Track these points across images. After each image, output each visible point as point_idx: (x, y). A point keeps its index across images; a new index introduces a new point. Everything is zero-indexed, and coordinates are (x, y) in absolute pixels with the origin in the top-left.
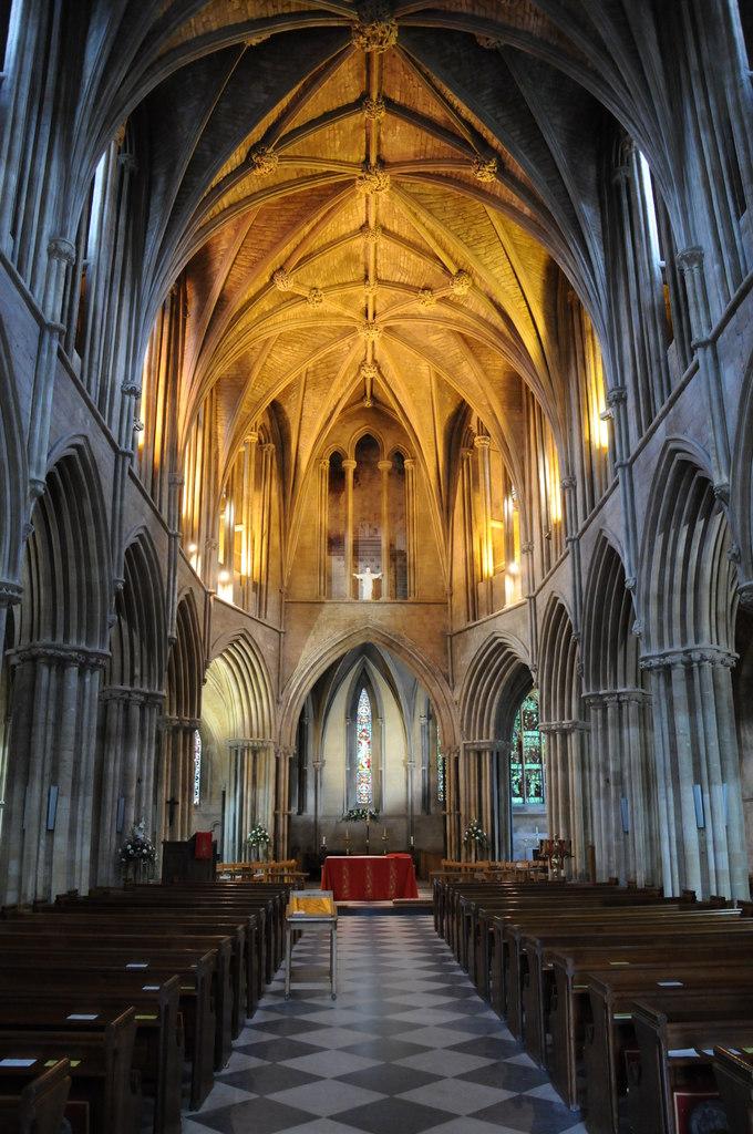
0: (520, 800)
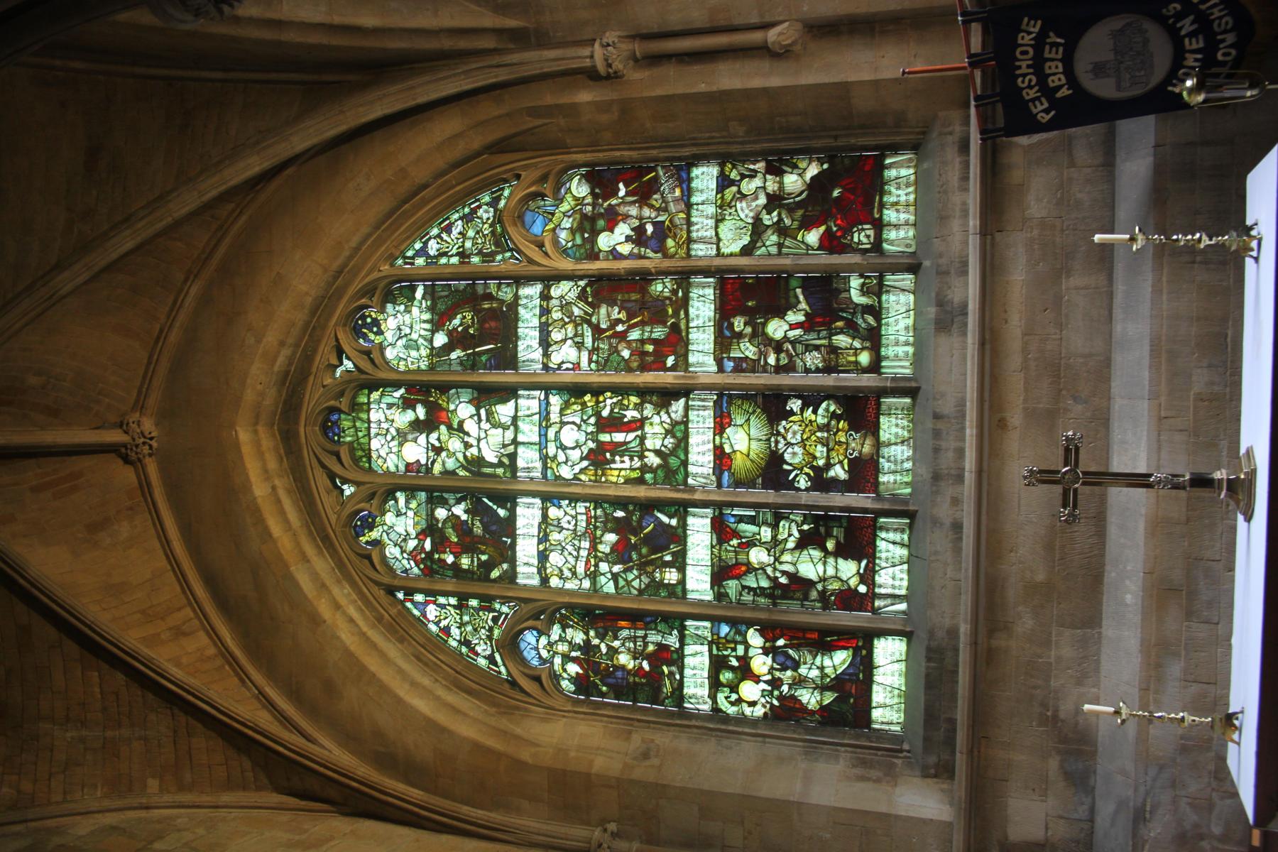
0: (889, 655)
